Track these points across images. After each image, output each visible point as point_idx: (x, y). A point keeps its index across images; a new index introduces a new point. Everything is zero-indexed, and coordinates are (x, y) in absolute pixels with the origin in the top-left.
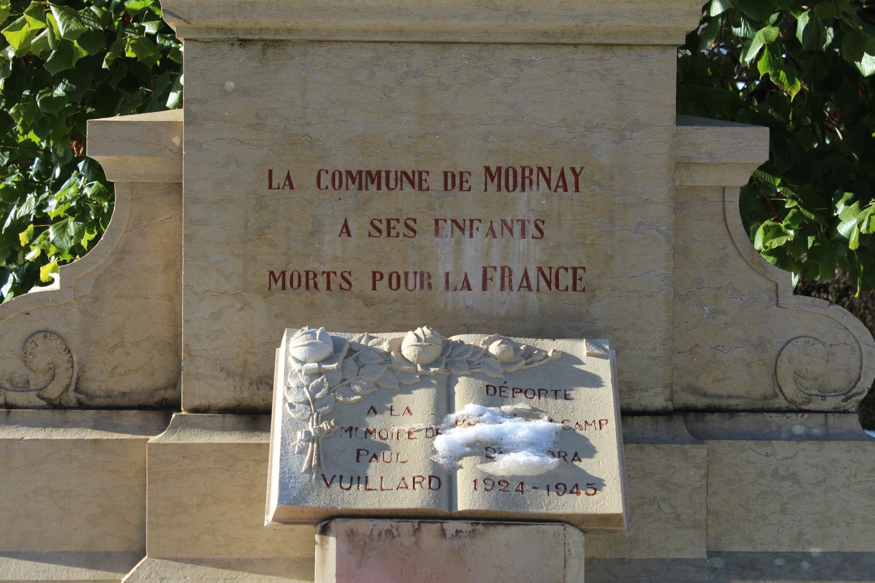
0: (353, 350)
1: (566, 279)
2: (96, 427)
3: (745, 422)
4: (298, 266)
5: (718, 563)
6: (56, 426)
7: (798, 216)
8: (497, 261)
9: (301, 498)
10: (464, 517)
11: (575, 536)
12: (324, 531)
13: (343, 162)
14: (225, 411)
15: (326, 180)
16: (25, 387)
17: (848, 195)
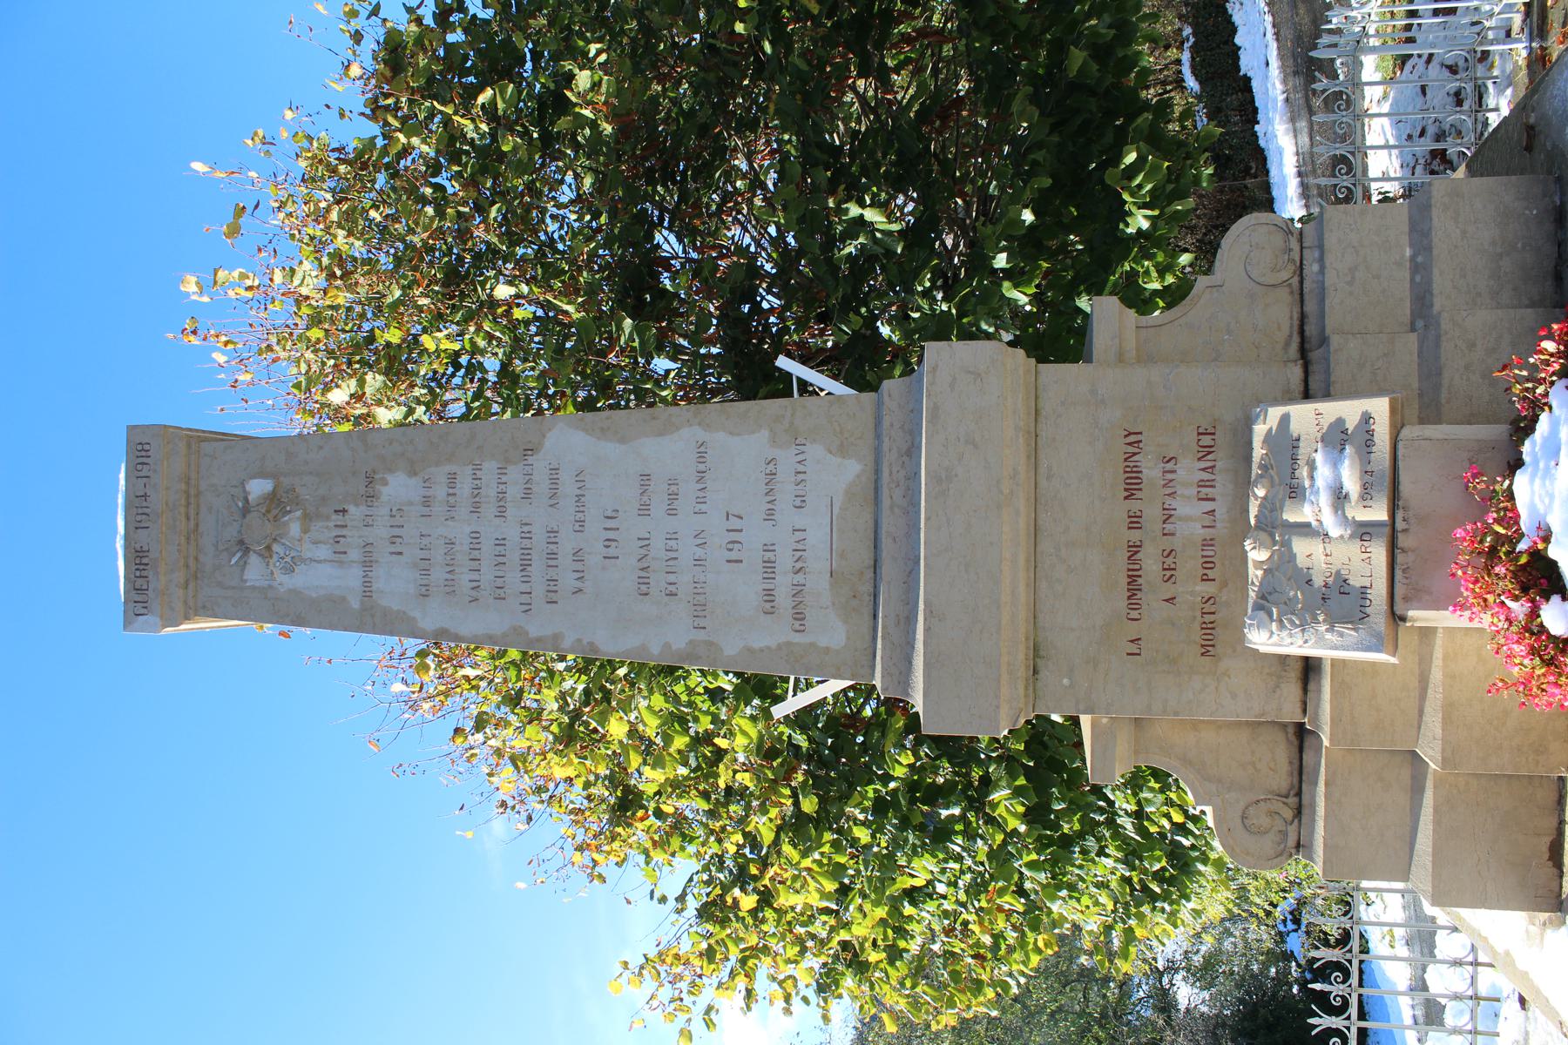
0: (1263, 596)
1: (1206, 440)
2: (1316, 783)
3: (1310, 307)
4: (1197, 635)
5: (1420, 324)
6: (1314, 812)
7: (1135, 260)
8: (1194, 491)
9: (1379, 636)
10: (1392, 515)
11: (1406, 433)
12: (1403, 619)
13: (1122, 603)
14: (1305, 690)
15: (1134, 614)
16: (1284, 834)
17: (1121, 226)
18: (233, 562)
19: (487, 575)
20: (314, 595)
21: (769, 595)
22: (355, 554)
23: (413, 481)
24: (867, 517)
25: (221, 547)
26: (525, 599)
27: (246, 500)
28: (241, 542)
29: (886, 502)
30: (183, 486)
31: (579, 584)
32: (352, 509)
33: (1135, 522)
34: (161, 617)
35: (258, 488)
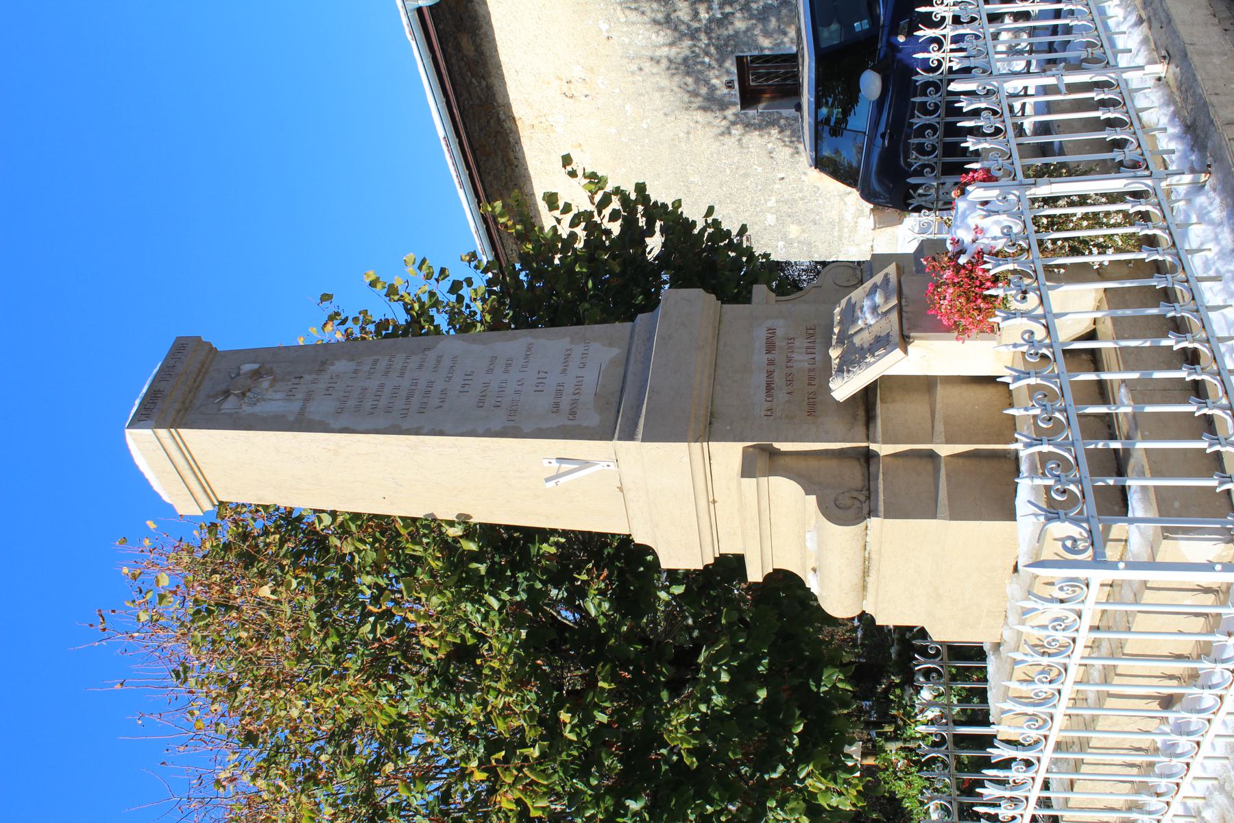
2: (877, 479)
20: (265, 415)
21: (557, 405)
23: (351, 363)
24: (621, 370)
33: (771, 362)
34: (156, 422)
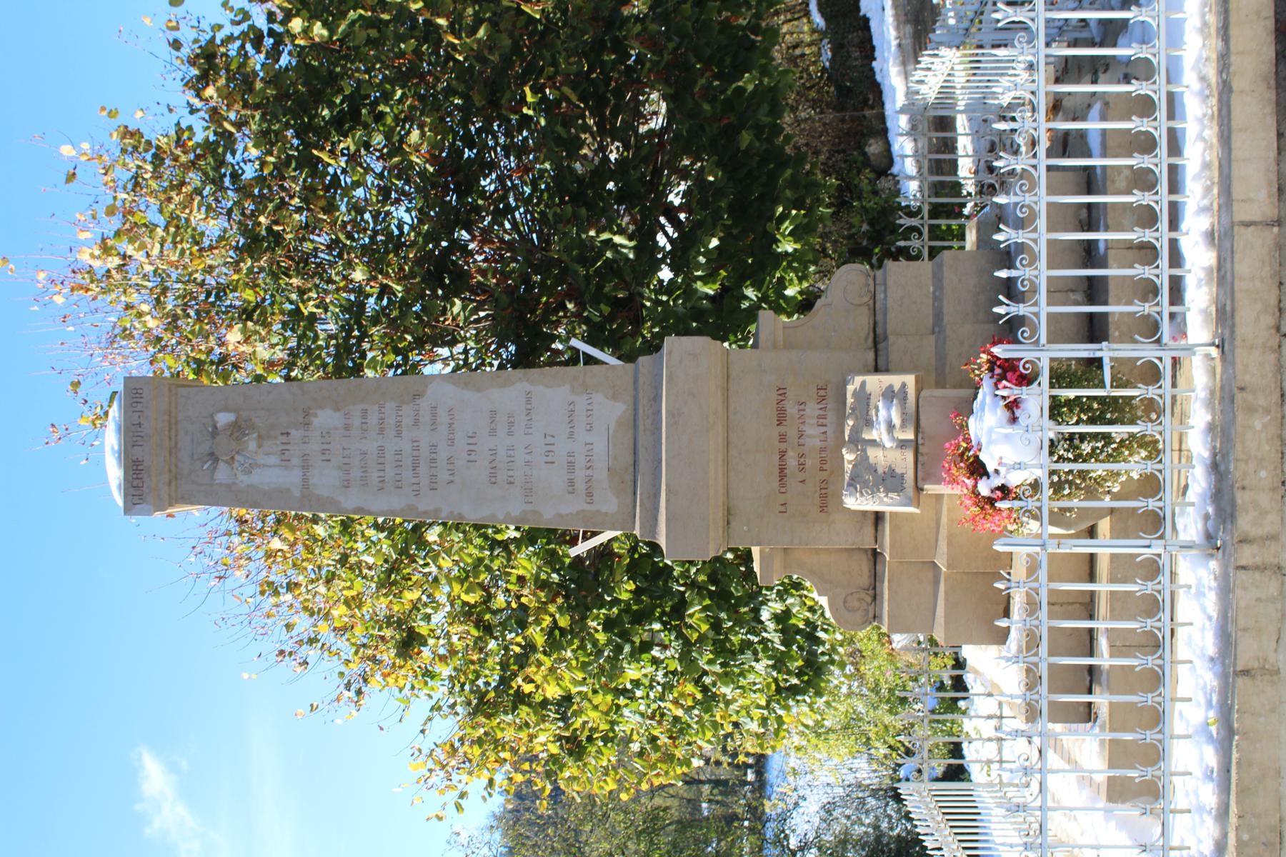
0: (852, 479)
1: (822, 393)
2: (883, 582)
3: (879, 318)
4: (817, 501)
5: (937, 329)
6: (882, 598)
7: (784, 270)
8: (815, 421)
9: (910, 499)
10: (916, 436)
11: (923, 393)
12: (922, 490)
13: (776, 484)
14: (876, 530)
15: (783, 490)
16: (867, 611)
17: (774, 246)
18: (205, 467)
19: (390, 473)
20: (267, 488)
21: (571, 482)
22: (296, 461)
23: (337, 414)
25: (195, 457)
26: (415, 487)
27: (215, 427)
28: (212, 454)
29: (641, 428)
30: (166, 418)
31: (451, 478)
32: (293, 432)
33: (783, 438)
35: (224, 419)
